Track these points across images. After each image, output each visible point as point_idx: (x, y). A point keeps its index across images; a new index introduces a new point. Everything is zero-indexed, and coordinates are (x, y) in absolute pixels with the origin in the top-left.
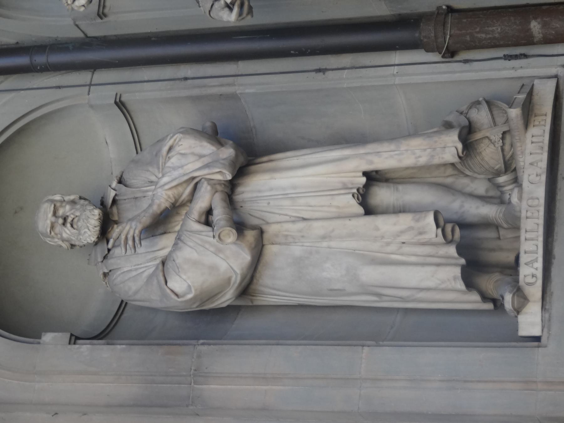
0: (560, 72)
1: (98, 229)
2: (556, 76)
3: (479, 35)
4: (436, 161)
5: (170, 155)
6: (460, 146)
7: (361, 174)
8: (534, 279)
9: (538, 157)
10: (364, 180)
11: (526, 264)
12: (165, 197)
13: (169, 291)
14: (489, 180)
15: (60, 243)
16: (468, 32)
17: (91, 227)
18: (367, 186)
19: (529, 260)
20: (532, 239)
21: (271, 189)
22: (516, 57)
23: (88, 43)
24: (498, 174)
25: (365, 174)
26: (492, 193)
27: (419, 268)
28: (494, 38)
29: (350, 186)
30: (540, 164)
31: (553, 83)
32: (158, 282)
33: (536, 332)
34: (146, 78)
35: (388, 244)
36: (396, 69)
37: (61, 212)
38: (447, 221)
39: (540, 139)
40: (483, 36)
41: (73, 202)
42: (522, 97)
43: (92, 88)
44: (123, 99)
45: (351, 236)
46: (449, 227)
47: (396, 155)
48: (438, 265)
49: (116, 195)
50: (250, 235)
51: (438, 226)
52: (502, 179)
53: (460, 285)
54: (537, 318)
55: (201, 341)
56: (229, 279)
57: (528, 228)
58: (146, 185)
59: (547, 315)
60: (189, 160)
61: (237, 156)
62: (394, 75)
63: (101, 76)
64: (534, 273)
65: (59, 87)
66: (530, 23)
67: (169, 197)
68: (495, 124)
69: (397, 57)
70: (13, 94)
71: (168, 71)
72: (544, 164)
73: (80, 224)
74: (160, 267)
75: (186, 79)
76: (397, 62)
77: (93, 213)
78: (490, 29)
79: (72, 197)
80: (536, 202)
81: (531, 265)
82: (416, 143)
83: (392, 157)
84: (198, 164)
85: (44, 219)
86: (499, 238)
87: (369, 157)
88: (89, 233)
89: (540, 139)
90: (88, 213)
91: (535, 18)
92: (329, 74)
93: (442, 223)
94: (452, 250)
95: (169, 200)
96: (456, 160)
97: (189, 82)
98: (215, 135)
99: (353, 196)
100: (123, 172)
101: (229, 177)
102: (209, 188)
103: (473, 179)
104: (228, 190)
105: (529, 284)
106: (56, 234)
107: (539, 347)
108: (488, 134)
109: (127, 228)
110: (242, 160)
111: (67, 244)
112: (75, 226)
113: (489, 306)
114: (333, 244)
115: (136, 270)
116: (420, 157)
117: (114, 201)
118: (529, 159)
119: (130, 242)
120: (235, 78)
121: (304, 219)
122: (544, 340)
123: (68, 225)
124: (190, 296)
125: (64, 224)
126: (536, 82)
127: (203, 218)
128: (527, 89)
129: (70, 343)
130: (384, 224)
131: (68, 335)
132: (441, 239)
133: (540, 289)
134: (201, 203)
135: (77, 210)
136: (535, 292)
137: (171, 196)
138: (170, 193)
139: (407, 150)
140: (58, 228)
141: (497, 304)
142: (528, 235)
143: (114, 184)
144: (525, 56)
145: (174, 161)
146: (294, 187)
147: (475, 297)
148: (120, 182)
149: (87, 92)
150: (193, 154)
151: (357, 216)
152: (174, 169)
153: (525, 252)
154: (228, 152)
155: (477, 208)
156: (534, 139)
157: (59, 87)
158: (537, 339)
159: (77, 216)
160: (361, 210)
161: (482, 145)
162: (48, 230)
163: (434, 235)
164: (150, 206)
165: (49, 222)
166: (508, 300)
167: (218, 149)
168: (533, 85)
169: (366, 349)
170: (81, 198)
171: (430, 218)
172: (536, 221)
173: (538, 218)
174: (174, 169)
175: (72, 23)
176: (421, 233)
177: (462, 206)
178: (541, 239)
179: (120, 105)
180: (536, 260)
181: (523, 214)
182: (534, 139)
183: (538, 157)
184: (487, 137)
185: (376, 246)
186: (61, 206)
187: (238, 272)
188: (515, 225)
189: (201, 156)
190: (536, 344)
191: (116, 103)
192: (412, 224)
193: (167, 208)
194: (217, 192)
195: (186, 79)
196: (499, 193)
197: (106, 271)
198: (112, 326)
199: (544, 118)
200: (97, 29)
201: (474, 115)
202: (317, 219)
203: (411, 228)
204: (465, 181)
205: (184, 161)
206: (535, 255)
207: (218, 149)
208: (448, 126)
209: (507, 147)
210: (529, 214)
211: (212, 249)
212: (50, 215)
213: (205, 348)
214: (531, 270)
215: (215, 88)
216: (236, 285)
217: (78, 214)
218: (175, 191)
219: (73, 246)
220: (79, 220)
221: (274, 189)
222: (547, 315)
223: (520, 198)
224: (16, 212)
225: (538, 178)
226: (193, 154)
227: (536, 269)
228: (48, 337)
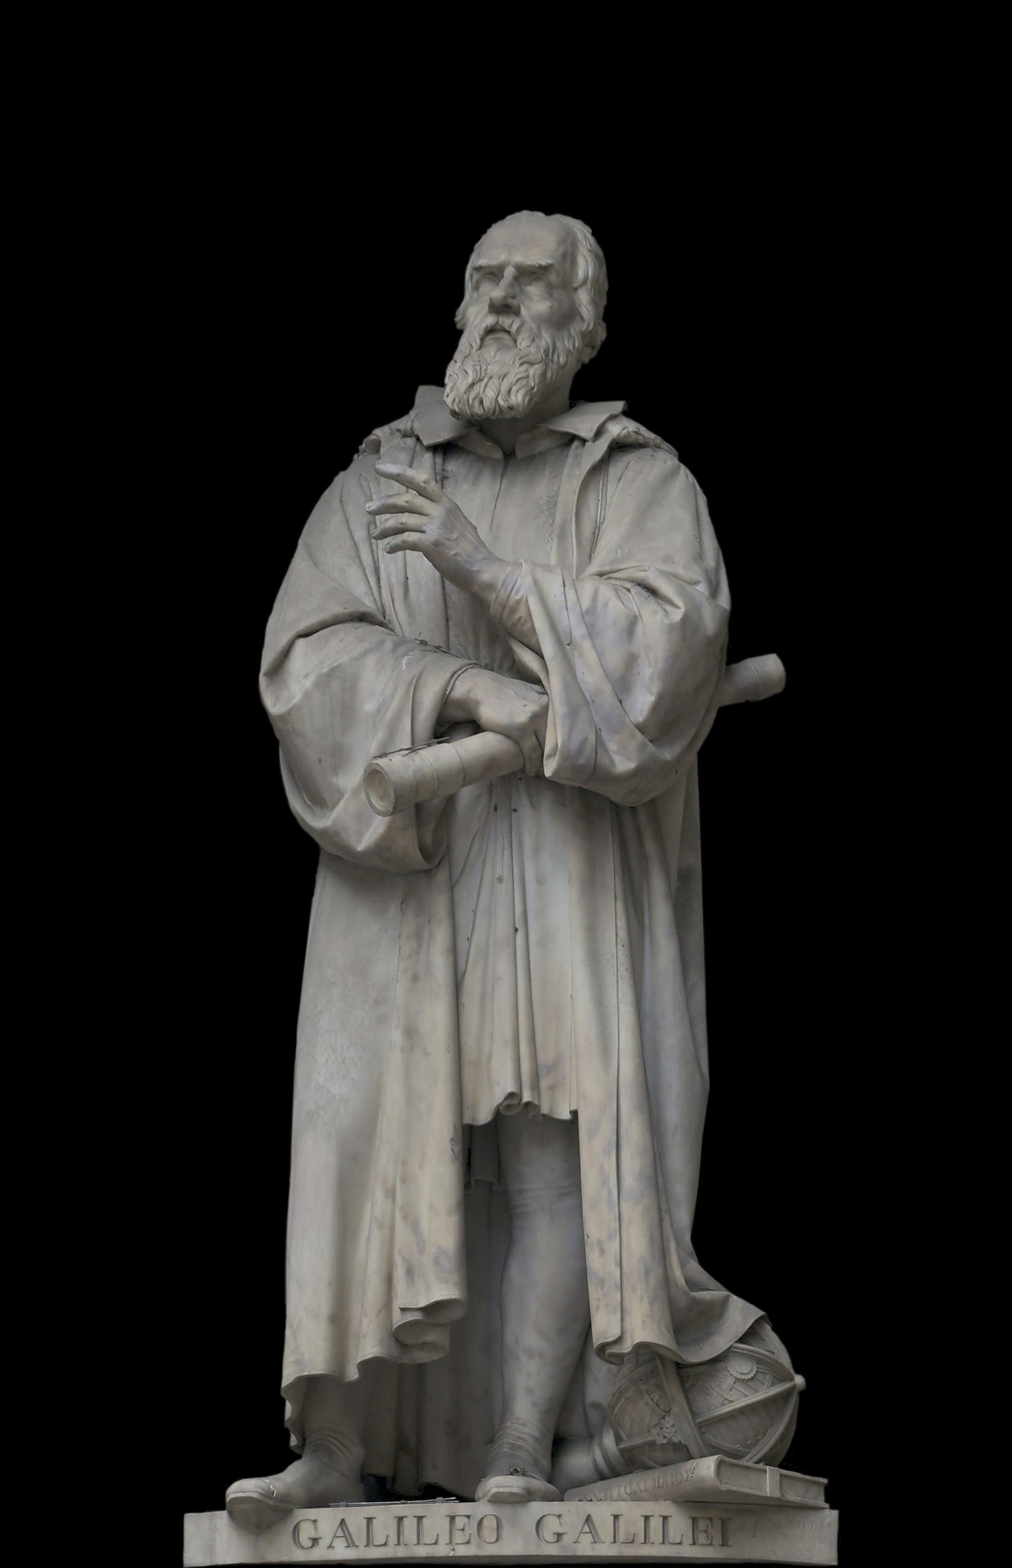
5: (635, 590)
8: (307, 1543)
9: (605, 1530)
11: (343, 1522)
12: (511, 602)
19: (352, 1529)
37: (534, 290)
39: (656, 1534)
47: (610, 1193)
64: (320, 1541)
67: (514, 610)
77: (514, 389)
80: (489, 1535)
81: (340, 1533)
83: (604, 1183)
90: (516, 372)
95: (506, 612)
105: (296, 1529)
116: (602, 1252)
132: (398, 1319)
137: (517, 616)
153: (370, 1520)
156: (656, 1523)
159: (515, 341)
172: (444, 1539)
180: (351, 1544)
182: (656, 1523)
183: (605, 1530)
186: (550, 288)
194: (517, 742)
199: (718, 1540)
205: (610, 637)
206: (361, 1541)
210: (460, 1522)
217: (523, 342)
223: (498, 1500)
225: (552, 1538)
227: (330, 1547)
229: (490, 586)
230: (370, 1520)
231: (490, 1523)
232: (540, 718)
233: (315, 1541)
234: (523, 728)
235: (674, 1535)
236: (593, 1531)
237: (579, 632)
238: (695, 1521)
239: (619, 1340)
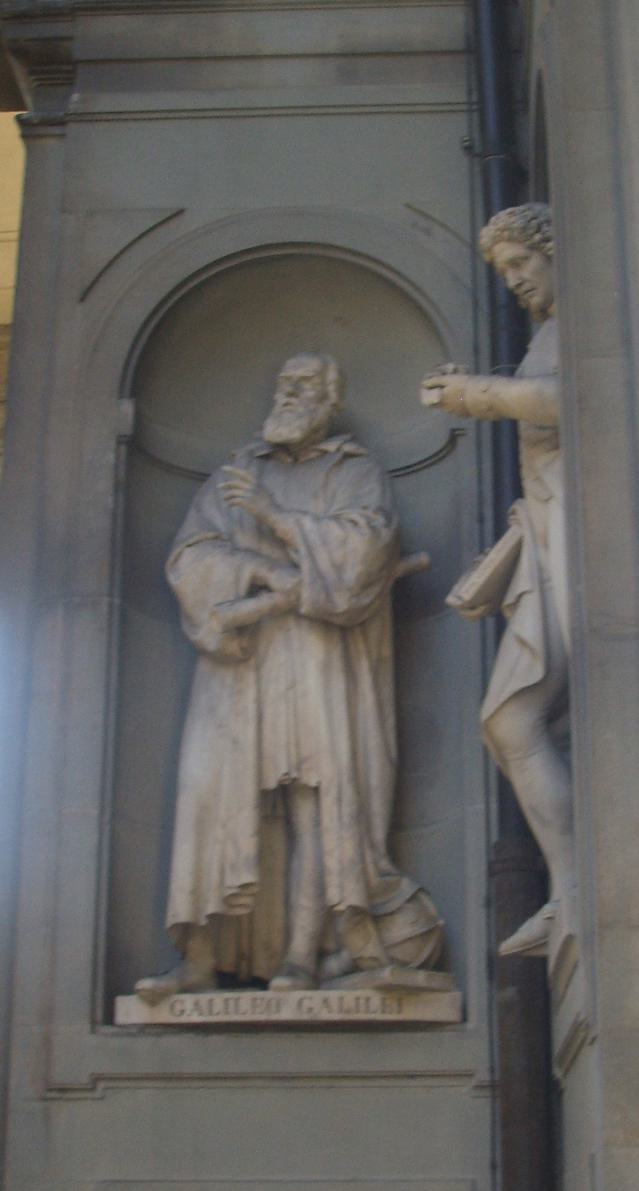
0: (471, 1025)
2: (464, 1018)
39: (362, 1007)
50: (234, 647)
59: (134, 1030)
82: (349, 849)
89: (362, 1007)
94: (212, 907)
99: (287, 774)
102: (289, 586)
105: (172, 1007)
127: (259, 583)
134: (279, 580)
136: (163, 1015)
142: (232, 1004)
145: (335, 531)
156: (362, 1002)
158: (109, 1017)
160: (271, 784)
182: (362, 1002)
210: (259, 1002)
213: (105, 608)
228: (127, 407)
230: (211, 1001)
233: (182, 1012)
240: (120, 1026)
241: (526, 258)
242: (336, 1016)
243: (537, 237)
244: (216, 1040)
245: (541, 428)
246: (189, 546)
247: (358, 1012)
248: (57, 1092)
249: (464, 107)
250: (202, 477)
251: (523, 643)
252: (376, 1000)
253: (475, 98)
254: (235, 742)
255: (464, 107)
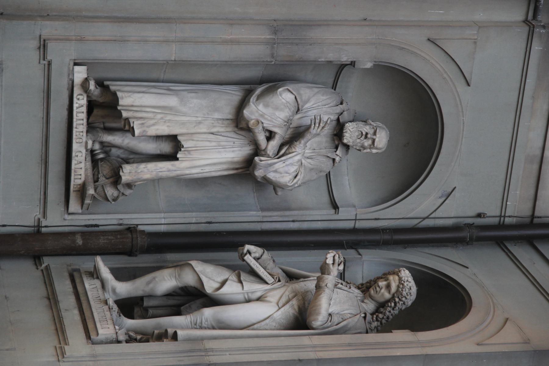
0: (66, 216)
1: (344, 131)
2: (69, 214)
3: (112, 238)
4: (135, 165)
6: (121, 173)
7: (180, 159)
9: (77, 166)
10: (178, 156)
13: (294, 93)
14: (109, 156)
15: (372, 123)
16: (118, 240)
17: (349, 132)
18: (177, 153)
19: (81, 108)
20: (80, 120)
21: (233, 151)
22: (92, 226)
23: (355, 245)
24: (102, 159)
25: (177, 159)
26: (108, 149)
27: (143, 104)
28: (103, 236)
29: (186, 152)
30: (76, 162)
31: (71, 210)
32: (301, 98)
33: (77, 68)
34: (319, 222)
35: (162, 118)
36: (163, 221)
37: (370, 142)
38: (128, 131)
39: (76, 177)
40: (110, 238)
41: (365, 148)
42: (87, 201)
43: (354, 218)
44: (334, 211)
45: (184, 124)
46: (127, 128)
48: (132, 106)
49: (336, 152)
51: (133, 128)
52: (101, 156)
53: (119, 94)
54: (76, 75)
55: (273, 63)
56: (257, 99)
57: (82, 126)
58: (314, 157)
60: (283, 170)
61: (253, 171)
62: (164, 218)
63: (349, 225)
65: (376, 219)
66: (83, 243)
67: (294, 148)
68: (103, 186)
69: (163, 228)
70: (408, 216)
71: (305, 226)
72: (74, 162)
73: (357, 134)
74: (300, 107)
75: (293, 221)
76: (163, 226)
78: (105, 241)
79: (365, 151)
80: (78, 141)
83: (161, 168)
84: (276, 166)
85: (382, 139)
86: (104, 123)
87: (174, 168)
88: (350, 128)
89: (76, 177)
91: (79, 246)
92: (204, 220)
93: (131, 130)
94: (125, 114)
96: (123, 166)
97: (291, 219)
98: (266, 182)
100: (333, 165)
101: (256, 158)
102: (268, 152)
103: (118, 157)
104: (259, 151)
105: (81, 95)
106: (373, 128)
107: (75, 60)
108: (107, 180)
109: (319, 130)
110: (251, 169)
111: (368, 123)
112: (360, 132)
113: (106, 83)
114: (194, 119)
115: (319, 106)
117: (337, 148)
118: (82, 165)
119: (317, 121)
120: (262, 220)
121: (212, 133)
122: (72, 64)
123: (364, 133)
124: (280, 90)
125: (367, 134)
126: (80, 211)
127: (273, 135)
128: (85, 206)
129: (355, 62)
130: (164, 130)
131: (356, 66)
132: (131, 121)
133: (74, 92)
134: (274, 144)
135: (359, 143)
136: (77, 91)
138: (294, 150)
139: (152, 172)
140: (371, 131)
141: (100, 83)
142: (81, 122)
143: (337, 159)
144: (86, 226)
145: (293, 169)
146: (219, 152)
147: (112, 88)
148: (334, 160)
149: (358, 216)
150: (281, 173)
151: (182, 134)
152: (292, 164)
153: (83, 112)
154: (259, 173)
155: (114, 140)
156: (79, 177)
157: (376, 219)
158: (76, 64)
160: (179, 138)
161: (110, 175)
162: (378, 130)
163: (135, 123)
164: (306, 143)
165: (378, 136)
166: (92, 85)
167: (265, 176)
168: (82, 209)
169: (173, 59)
170: (360, 150)
171: (137, 132)
173: (76, 131)
174: (292, 164)
175: (363, 256)
176: (143, 124)
177: (123, 140)
178: (74, 120)
179: (335, 206)
180: (77, 108)
181: (85, 134)
182: (79, 177)
183: (77, 166)
184: (107, 179)
185: (169, 117)
186: (370, 145)
187: (251, 103)
188: (91, 128)
189: (276, 171)
190: (76, 61)
191: (338, 208)
192: (147, 129)
193: (296, 141)
194: (264, 150)
195: (293, 221)
196: (104, 149)
197: (340, 106)
198: (338, 73)
199: (75, 189)
200: (351, 253)
201: (116, 194)
202: (205, 133)
203: (149, 127)
204: (123, 156)
205: (286, 169)
206: (78, 110)
207: (265, 176)
208: (129, 186)
209: (96, 173)
210: (81, 134)
211: (266, 116)
212: (377, 140)
214: (80, 103)
215: (275, 215)
216: (254, 96)
217: (358, 141)
218: (290, 151)
219: (365, 122)
220: (358, 136)
221: (233, 151)
222: (71, 77)
223: (86, 143)
224: (408, 143)
225: (77, 154)
226: (281, 173)
228: (369, 65)
229: (300, 143)
230: (83, 112)
231: (81, 141)
232: (269, 156)
233: (78, 99)
234: (266, 152)
235: (76, 181)
236: (78, 164)
237: (287, 163)
238: (80, 185)
239: (123, 172)
240: (73, 68)
241: (389, 292)
242: (73, 167)
243: (397, 300)
244: (65, 113)
245: (309, 304)
246: (296, 98)
247: (75, 175)
248: (43, 46)
249: (503, 214)
250: (334, 87)
251: (223, 283)
252: (80, 182)
253: (508, 220)
254: (200, 123)
255: (503, 214)
